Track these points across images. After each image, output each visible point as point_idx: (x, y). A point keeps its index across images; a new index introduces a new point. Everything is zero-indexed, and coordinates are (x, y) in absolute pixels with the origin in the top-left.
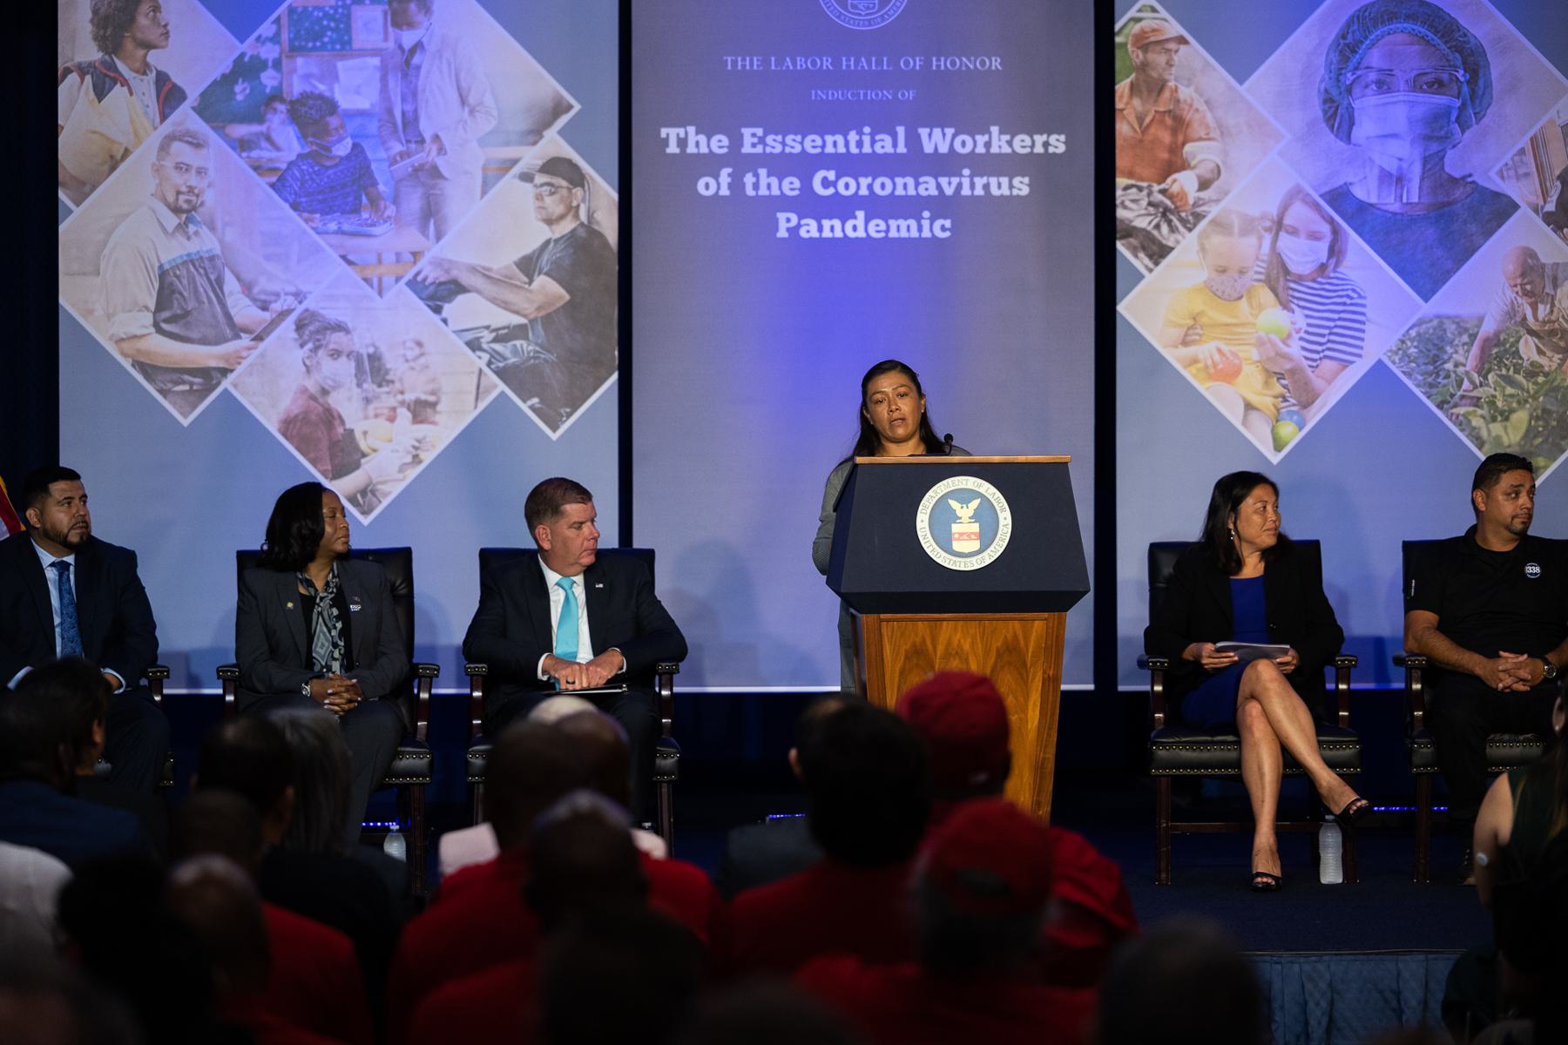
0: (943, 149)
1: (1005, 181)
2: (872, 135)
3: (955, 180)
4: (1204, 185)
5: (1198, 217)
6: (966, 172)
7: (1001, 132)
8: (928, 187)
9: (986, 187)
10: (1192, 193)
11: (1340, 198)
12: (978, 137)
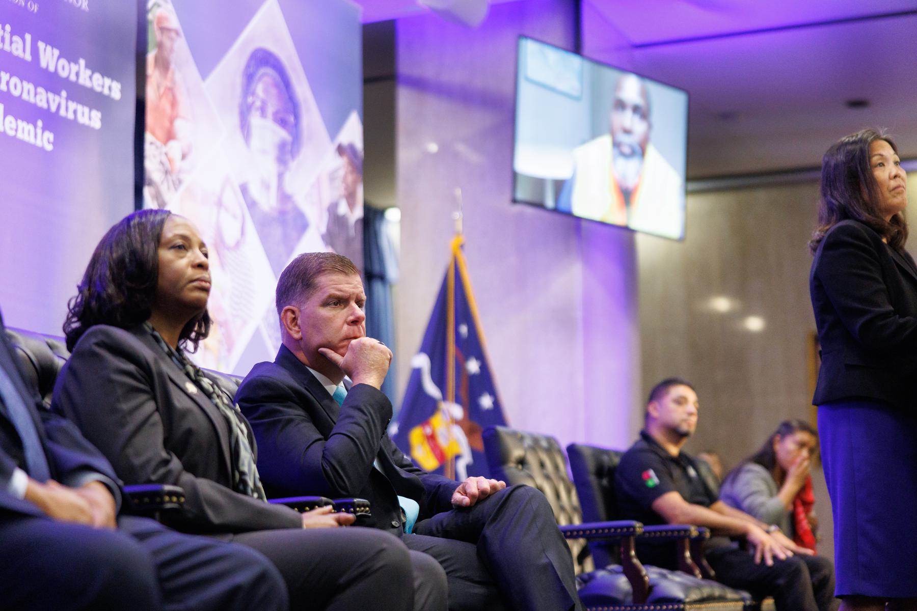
0: (52, 69)
1: (86, 110)
2: (12, 33)
3: (57, 98)
4: (184, 157)
5: (180, 182)
6: (64, 94)
7: (87, 66)
8: (42, 98)
9: (75, 112)
10: (178, 163)
11: (244, 189)
12: (72, 65)
